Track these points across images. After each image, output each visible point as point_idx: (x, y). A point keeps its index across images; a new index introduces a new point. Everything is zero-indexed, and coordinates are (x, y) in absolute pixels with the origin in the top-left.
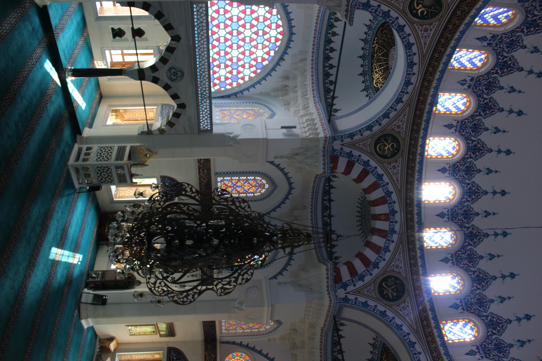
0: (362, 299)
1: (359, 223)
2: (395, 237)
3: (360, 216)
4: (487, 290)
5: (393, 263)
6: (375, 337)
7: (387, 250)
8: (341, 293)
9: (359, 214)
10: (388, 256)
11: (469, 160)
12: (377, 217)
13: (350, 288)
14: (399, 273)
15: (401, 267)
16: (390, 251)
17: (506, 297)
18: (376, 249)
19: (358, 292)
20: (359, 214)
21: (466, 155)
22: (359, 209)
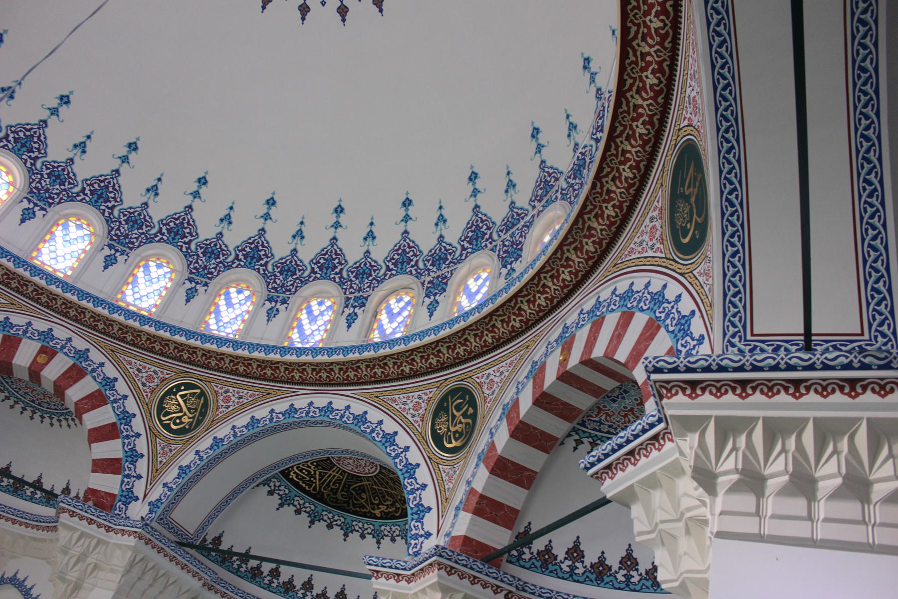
0: (171, 475)
1: (47, 421)
2: (96, 356)
3: (34, 412)
4: (273, 252)
5: (140, 384)
6: (267, 488)
7: (110, 383)
8: (138, 510)
9: (28, 413)
10: (122, 387)
11: (39, 164)
12: (35, 372)
13: (139, 488)
14: (163, 380)
15: (155, 372)
16: (116, 379)
17: (298, 228)
18: (96, 400)
19: (155, 472)
20: (28, 413)
21: (25, 163)
22: (18, 408)
